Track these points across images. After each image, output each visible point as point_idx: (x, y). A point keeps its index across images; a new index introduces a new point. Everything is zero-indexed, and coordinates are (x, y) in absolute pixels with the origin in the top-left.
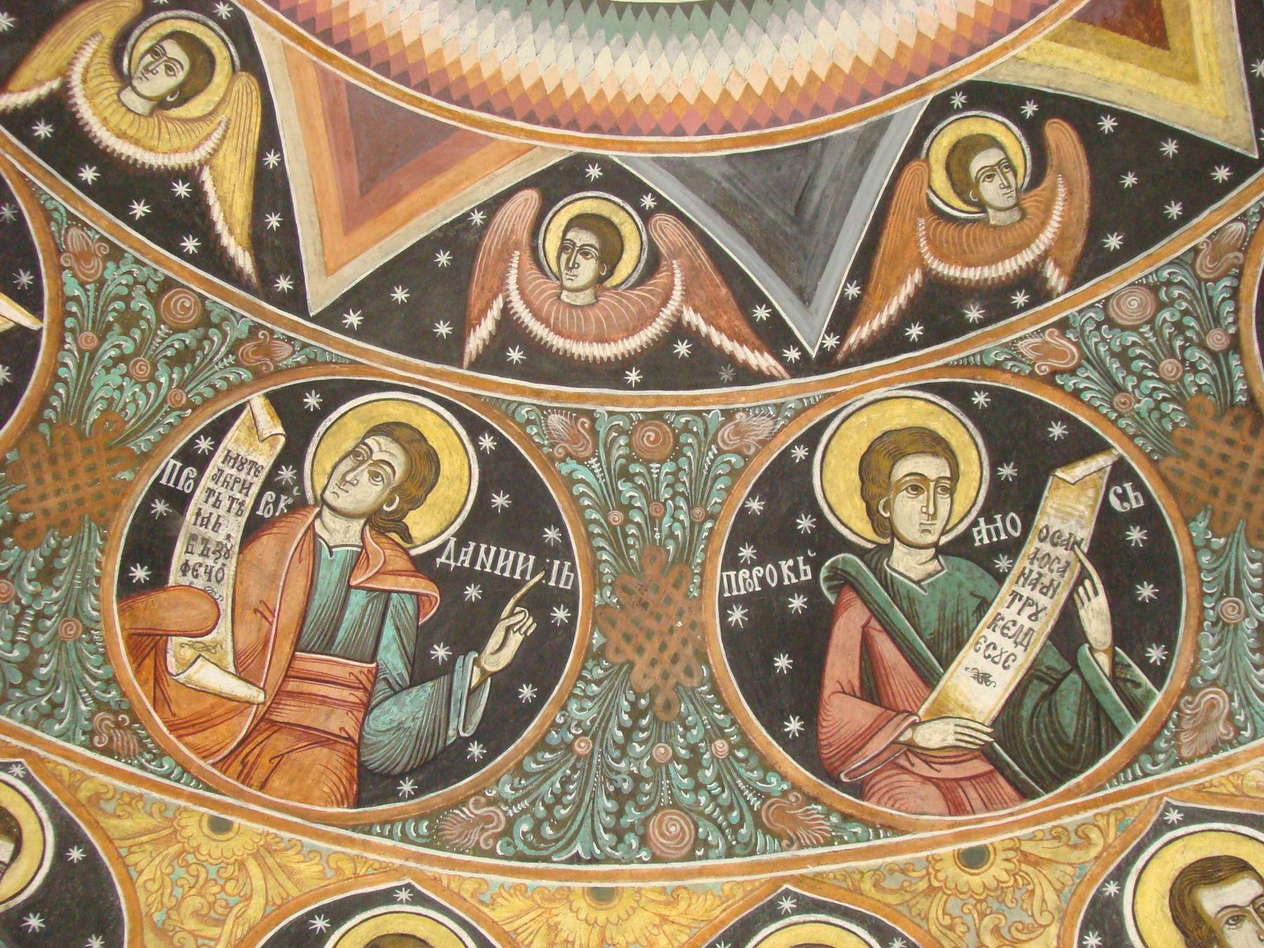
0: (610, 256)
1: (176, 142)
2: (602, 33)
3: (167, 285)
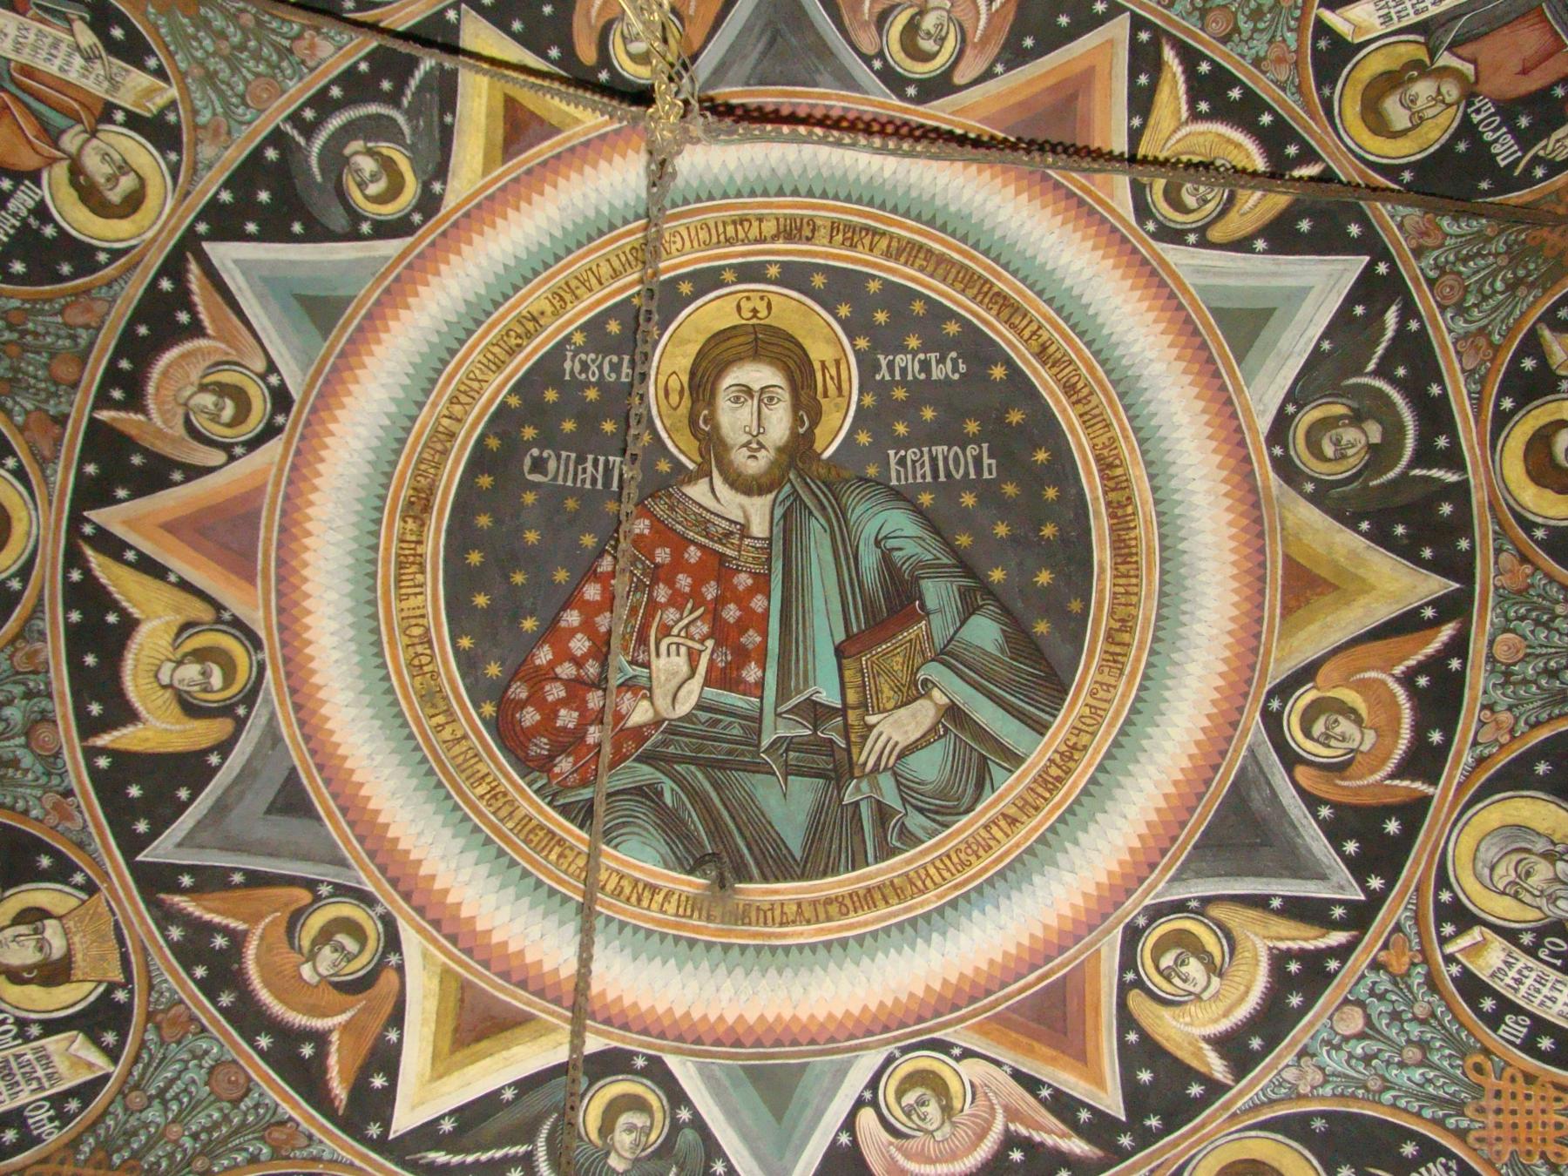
0: (912, 28)
1: (1201, 139)
2: (887, 187)
3: (1225, 40)
